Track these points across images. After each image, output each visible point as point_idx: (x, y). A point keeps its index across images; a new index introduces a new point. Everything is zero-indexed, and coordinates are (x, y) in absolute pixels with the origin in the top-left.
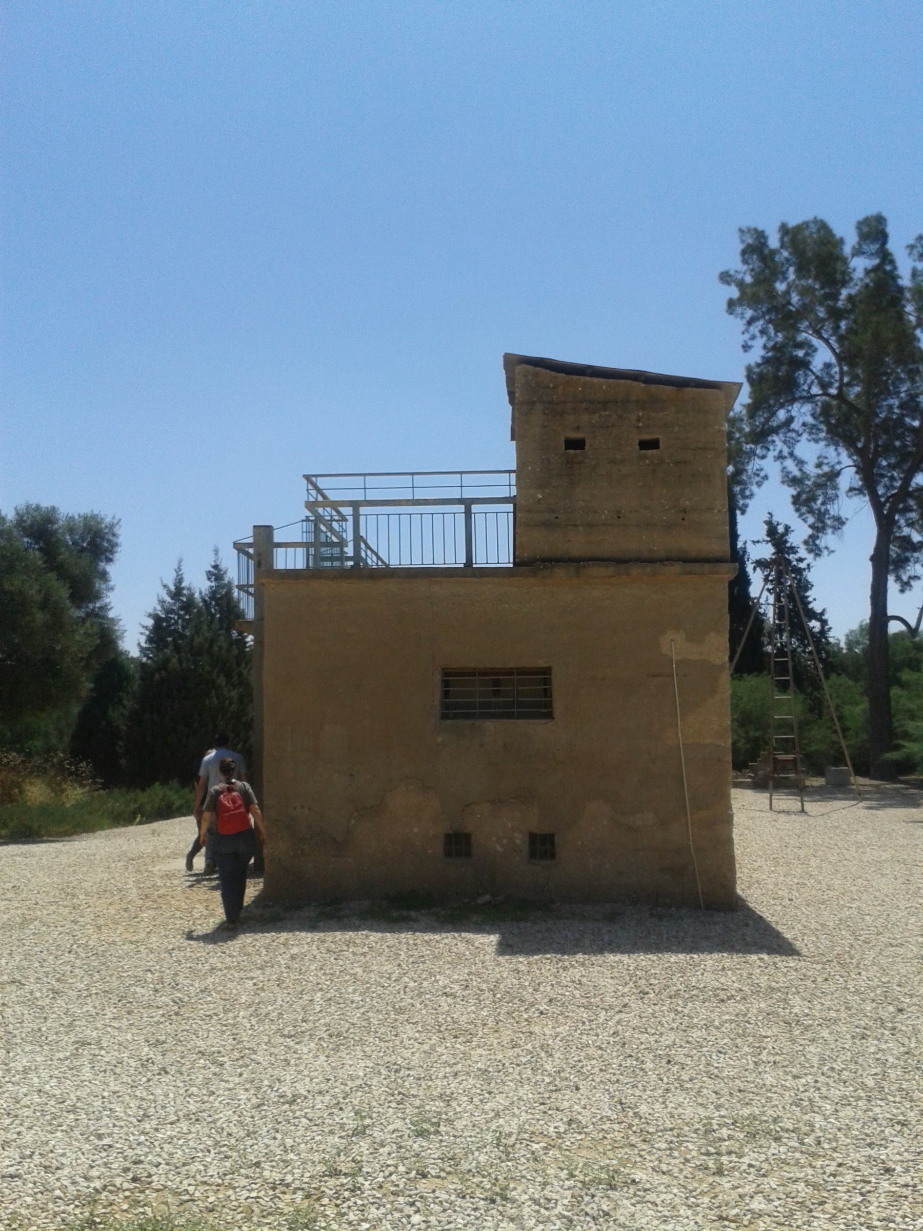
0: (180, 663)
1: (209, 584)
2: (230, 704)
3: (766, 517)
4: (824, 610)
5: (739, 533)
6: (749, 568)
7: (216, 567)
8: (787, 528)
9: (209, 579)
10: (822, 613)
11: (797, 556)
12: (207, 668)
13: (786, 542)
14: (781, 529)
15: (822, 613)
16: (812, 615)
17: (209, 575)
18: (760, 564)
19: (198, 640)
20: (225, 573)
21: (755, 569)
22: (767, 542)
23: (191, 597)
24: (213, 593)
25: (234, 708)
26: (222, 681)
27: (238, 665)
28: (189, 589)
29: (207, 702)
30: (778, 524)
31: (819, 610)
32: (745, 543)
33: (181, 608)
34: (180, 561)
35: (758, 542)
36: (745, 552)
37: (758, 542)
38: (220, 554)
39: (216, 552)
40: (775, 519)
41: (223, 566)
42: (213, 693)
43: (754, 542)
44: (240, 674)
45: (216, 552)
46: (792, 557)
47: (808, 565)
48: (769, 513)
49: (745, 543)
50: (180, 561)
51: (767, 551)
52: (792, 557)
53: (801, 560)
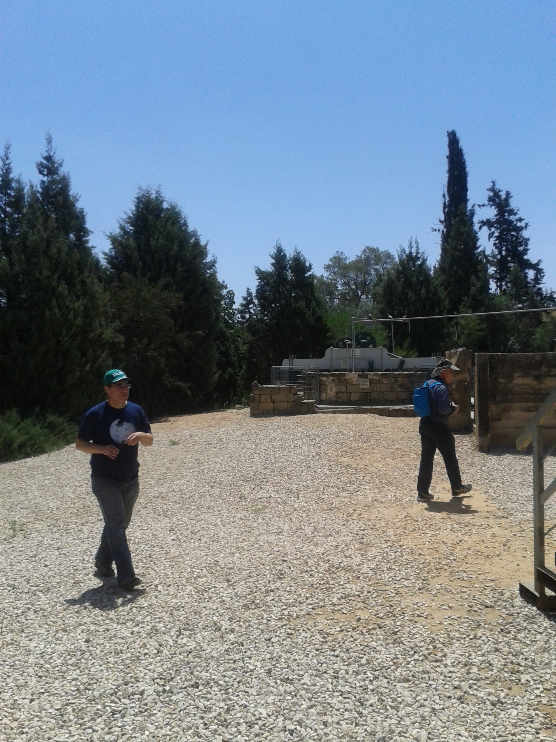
0: (11, 265)
1: (41, 177)
2: (76, 317)
3: (490, 185)
4: (539, 261)
5: (468, 197)
6: (476, 227)
7: (49, 158)
8: (508, 194)
9: (41, 172)
10: (538, 264)
11: (517, 217)
12: (46, 273)
13: (508, 205)
14: (503, 195)
15: (538, 264)
16: (529, 265)
17: (41, 168)
18: (488, 223)
19: (32, 238)
20: (61, 165)
21: (480, 228)
22: (492, 205)
23: (20, 191)
24: (46, 188)
25: (79, 321)
26: (63, 288)
27: (81, 272)
28: (18, 182)
29: (47, 313)
30: (500, 191)
31: (534, 261)
32: (473, 206)
33: (9, 204)
34: (8, 148)
35: (484, 205)
36: (473, 214)
37: (484, 205)
38: (53, 143)
39: (49, 141)
40: (498, 187)
41: (57, 158)
42: (54, 302)
43: (479, 206)
44: (83, 283)
45: (49, 141)
46: (512, 218)
47: (526, 224)
48: (493, 182)
49: (473, 206)
50: (8, 148)
51: (491, 213)
52: (512, 218)
53: (520, 220)
